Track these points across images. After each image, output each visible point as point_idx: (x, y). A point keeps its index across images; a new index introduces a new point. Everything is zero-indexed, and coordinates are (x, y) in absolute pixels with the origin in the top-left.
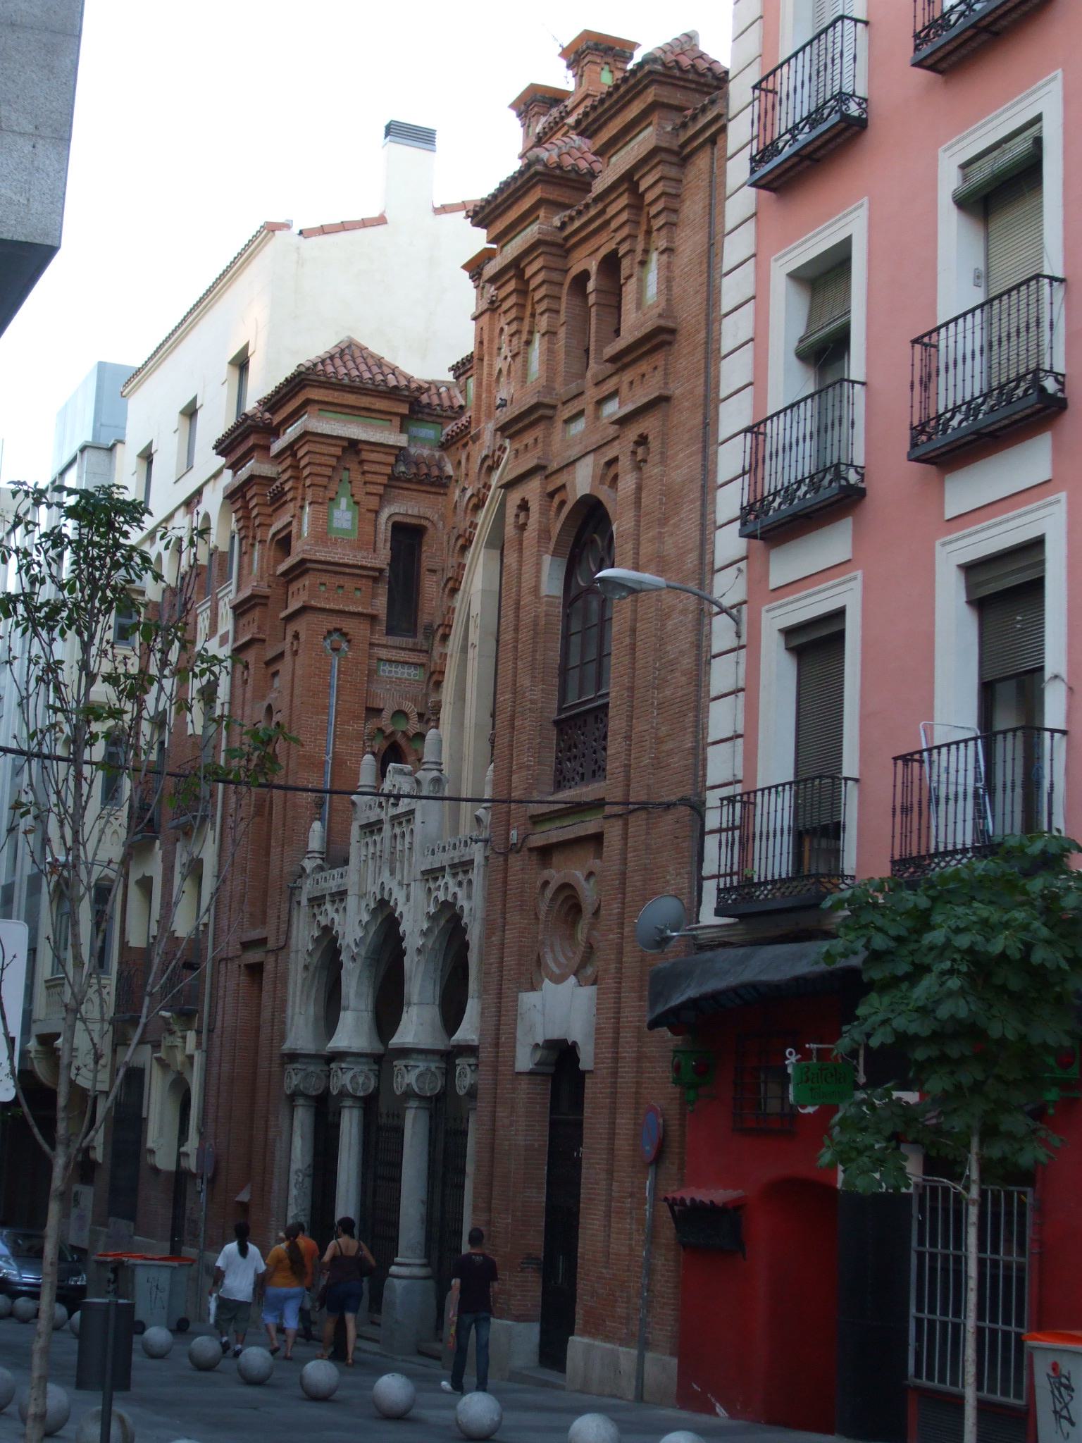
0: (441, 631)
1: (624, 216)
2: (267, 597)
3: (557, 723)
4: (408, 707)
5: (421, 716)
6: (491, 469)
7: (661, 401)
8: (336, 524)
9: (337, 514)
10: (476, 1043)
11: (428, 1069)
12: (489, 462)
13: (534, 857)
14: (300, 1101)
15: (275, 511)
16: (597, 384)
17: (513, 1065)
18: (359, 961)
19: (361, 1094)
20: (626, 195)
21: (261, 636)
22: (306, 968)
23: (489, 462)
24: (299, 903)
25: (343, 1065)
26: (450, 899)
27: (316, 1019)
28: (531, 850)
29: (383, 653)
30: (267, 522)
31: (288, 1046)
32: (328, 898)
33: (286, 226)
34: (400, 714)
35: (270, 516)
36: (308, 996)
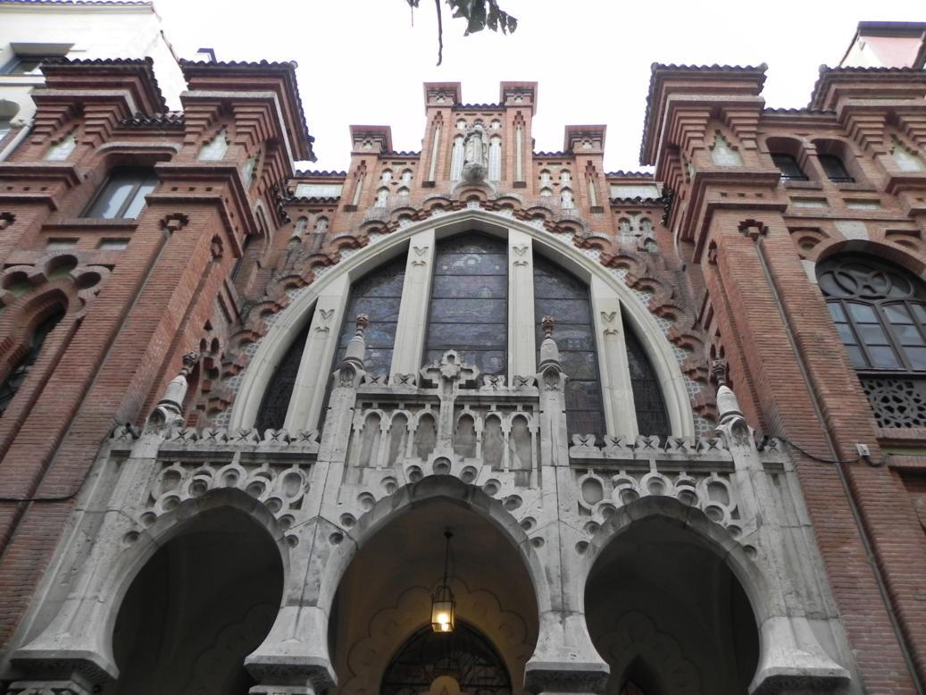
0: (267, 306)
2: (77, 182)
4: (221, 341)
5: (223, 357)
6: (375, 231)
12: (380, 226)
15: (115, 135)
18: (346, 546)
21: (57, 204)
22: (133, 536)
23: (380, 226)
30: (105, 137)
32: (237, 457)
33: (160, 19)
34: (215, 343)
35: (109, 136)
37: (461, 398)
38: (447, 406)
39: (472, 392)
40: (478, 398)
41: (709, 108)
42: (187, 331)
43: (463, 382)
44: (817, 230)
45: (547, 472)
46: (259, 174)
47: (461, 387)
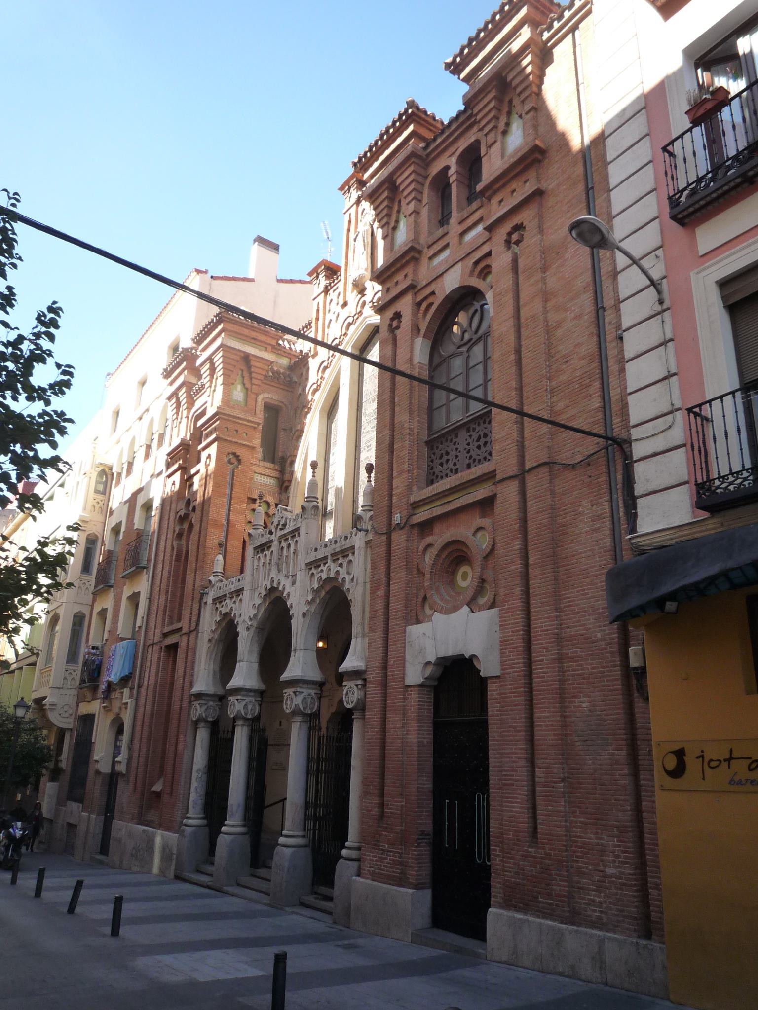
1: (492, 104)
3: (427, 443)
7: (539, 194)
8: (234, 398)
9: (235, 392)
10: (363, 668)
11: (309, 695)
12: (325, 364)
13: (416, 532)
14: (202, 725)
16: (460, 223)
17: (403, 681)
18: (252, 630)
19: (249, 716)
20: (494, 91)
22: (210, 640)
23: (325, 364)
24: (206, 603)
25: (239, 697)
26: (332, 575)
27: (214, 672)
28: (412, 526)
29: (257, 469)
31: (196, 689)
36: (210, 658)
37: (281, 537)
38: (275, 543)
39: (283, 532)
40: (285, 535)
41: (384, 188)
42: (232, 517)
43: (280, 527)
44: (433, 293)
45: (298, 573)
46: (248, 385)
47: (281, 529)
